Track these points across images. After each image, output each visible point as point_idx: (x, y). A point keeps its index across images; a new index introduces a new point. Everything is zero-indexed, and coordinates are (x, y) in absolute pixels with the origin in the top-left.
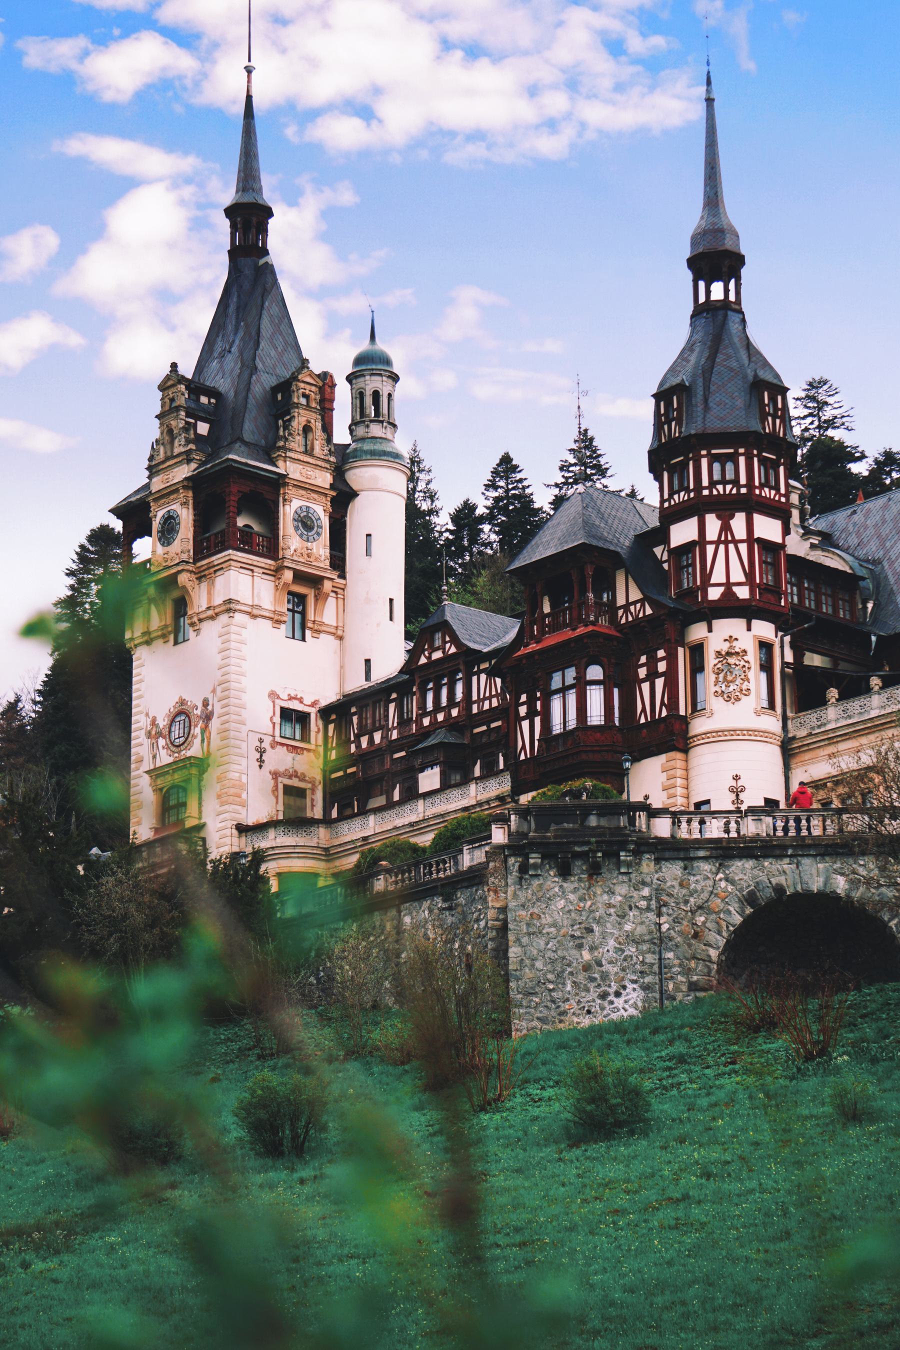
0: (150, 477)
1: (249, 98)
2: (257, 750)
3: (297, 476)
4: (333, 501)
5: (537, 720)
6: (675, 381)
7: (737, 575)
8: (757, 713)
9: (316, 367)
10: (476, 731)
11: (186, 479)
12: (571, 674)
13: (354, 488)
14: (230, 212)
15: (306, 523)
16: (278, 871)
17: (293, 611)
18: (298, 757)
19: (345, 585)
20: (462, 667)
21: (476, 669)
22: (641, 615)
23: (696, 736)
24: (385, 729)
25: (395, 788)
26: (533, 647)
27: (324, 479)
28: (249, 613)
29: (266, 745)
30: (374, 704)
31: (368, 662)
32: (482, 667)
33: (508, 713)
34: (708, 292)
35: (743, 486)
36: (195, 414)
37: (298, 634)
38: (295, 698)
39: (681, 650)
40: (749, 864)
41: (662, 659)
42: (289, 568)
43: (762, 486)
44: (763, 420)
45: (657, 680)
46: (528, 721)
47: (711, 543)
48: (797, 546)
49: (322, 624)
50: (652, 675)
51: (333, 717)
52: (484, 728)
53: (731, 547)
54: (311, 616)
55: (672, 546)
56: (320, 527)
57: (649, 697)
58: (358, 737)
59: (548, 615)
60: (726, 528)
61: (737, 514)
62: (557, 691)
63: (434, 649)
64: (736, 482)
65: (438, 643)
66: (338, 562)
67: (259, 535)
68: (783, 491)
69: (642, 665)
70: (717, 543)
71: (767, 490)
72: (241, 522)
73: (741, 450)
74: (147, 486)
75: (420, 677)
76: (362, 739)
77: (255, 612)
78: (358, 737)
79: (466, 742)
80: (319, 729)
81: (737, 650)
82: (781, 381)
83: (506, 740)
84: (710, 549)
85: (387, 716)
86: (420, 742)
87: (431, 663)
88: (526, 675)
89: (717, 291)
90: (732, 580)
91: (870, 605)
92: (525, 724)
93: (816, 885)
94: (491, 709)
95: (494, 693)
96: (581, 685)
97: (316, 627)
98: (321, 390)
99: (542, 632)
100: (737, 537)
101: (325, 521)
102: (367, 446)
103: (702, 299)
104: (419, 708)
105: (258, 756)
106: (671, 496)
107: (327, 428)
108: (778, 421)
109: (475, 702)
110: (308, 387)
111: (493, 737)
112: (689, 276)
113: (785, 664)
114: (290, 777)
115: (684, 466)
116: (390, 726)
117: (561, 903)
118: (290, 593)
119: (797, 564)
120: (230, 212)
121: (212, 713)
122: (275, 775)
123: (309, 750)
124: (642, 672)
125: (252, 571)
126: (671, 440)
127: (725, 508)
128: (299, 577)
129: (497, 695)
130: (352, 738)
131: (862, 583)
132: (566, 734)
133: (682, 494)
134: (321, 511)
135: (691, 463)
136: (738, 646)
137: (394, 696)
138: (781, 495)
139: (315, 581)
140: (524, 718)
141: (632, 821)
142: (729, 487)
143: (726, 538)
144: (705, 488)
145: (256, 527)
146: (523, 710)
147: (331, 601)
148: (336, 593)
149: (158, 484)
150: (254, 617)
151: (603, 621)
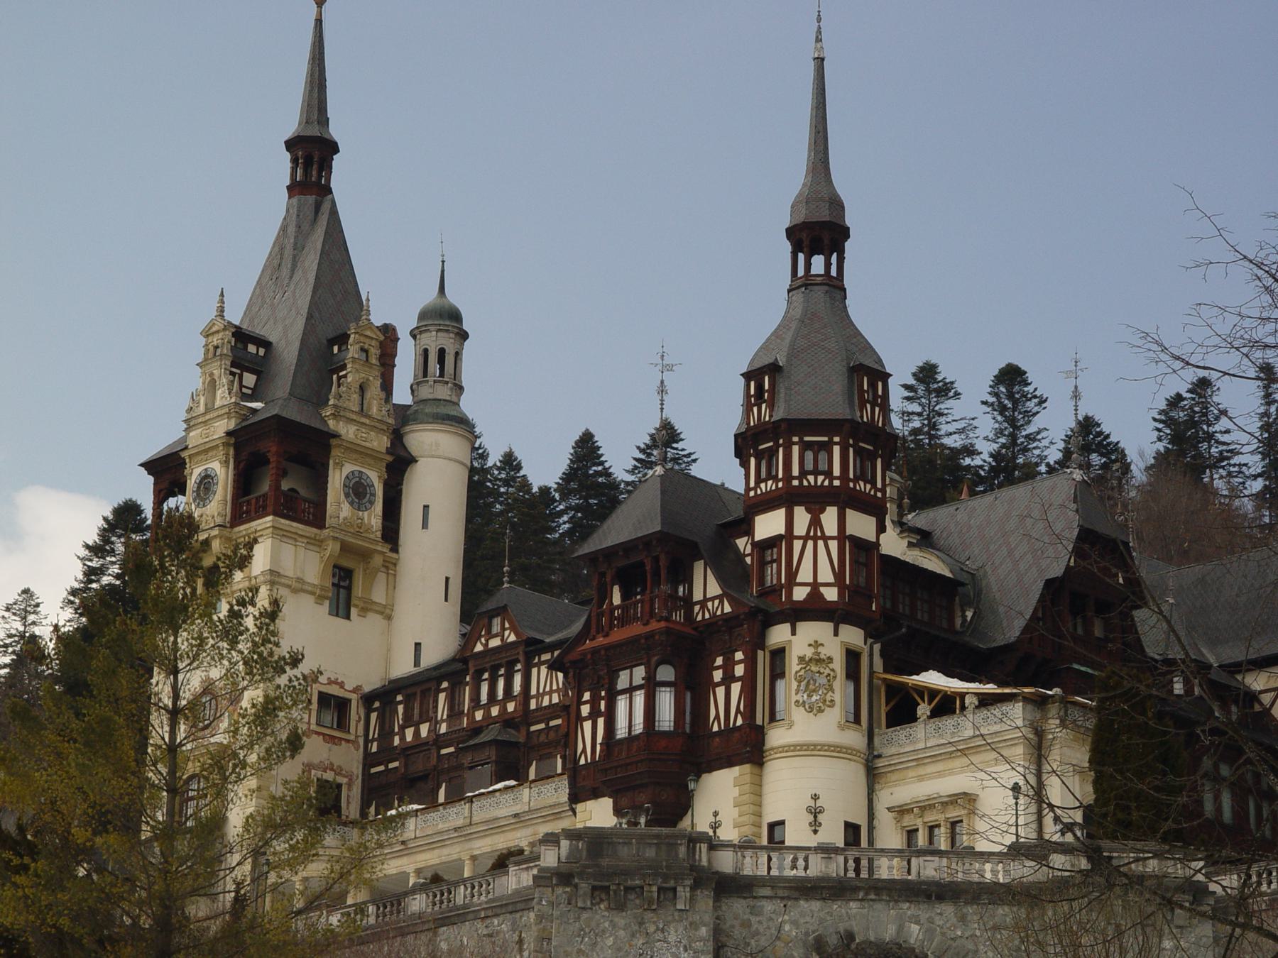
0: (187, 430)
1: (319, 22)
3: (351, 436)
4: (390, 467)
5: (601, 721)
6: (768, 360)
7: (826, 575)
8: (841, 727)
9: (378, 318)
10: (533, 728)
11: (229, 434)
12: (639, 673)
14: (290, 145)
15: (358, 491)
18: (335, 748)
20: (521, 658)
22: (719, 613)
23: (772, 749)
25: (439, 787)
26: (601, 640)
27: (380, 443)
28: (289, 586)
31: (418, 645)
33: (568, 711)
34: (808, 265)
35: (837, 478)
36: (239, 364)
38: (336, 682)
39: (760, 653)
40: (815, 905)
41: (740, 662)
42: (335, 538)
43: (856, 480)
44: (862, 407)
45: (733, 685)
46: (590, 722)
47: (799, 538)
48: (893, 544)
50: (729, 679)
51: (377, 704)
52: (542, 726)
53: (820, 543)
54: (358, 590)
55: (757, 539)
56: (374, 495)
57: (725, 704)
58: (403, 728)
59: (618, 607)
60: (816, 522)
61: (828, 508)
62: (623, 692)
63: (490, 636)
64: (828, 474)
65: (496, 628)
66: (391, 533)
67: (306, 500)
68: (879, 485)
69: (718, 668)
70: (805, 539)
71: (862, 484)
72: (285, 486)
73: (837, 439)
74: (184, 439)
77: (294, 585)
78: (403, 728)
79: (522, 740)
81: (822, 656)
82: (883, 366)
83: (567, 740)
84: (797, 545)
85: (436, 707)
86: (471, 737)
87: (488, 652)
88: (591, 673)
89: (818, 264)
90: (820, 580)
91: (969, 614)
92: (587, 725)
93: (889, 933)
94: (551, 706)
95: (555, 687)
96: (651, 686)
98: (382, 345)
99: (611, 626)
100: (827, 534)
102: (429, 409)
103: (801, 272)
104: (471, 700)
107: (387, 387)
108: (877, 409)
109: (534, 697)
110: (367, 341)
112: (787, 247)
113: (872, 673)
115: (772, 453)
117: (610, 941)
119: (891, 563)
120: (290, 145)
123: (348, 741)
124: (718, 675)
125: (296, 540)
126: (760, 423)
127: (815, 500)
129: (558, 690)
131: (960, 589)
132: (631, 739)
133: (770, 483)
134: (375, 478)
135: (781, 450)
136: (824, 652)
137: (445, 685)
138: (877, 490)
139: (365, 556)
140: (586, 719)
141: (692, 851)
142: (820, 478)
143: (815, 533)
144: (795, 478)
145: (303, 492)
146: (585, 710)
147: (381, 577)
148: (387, 568)
149: (195, 438)
150: (295, 591)
151: (678, 616)
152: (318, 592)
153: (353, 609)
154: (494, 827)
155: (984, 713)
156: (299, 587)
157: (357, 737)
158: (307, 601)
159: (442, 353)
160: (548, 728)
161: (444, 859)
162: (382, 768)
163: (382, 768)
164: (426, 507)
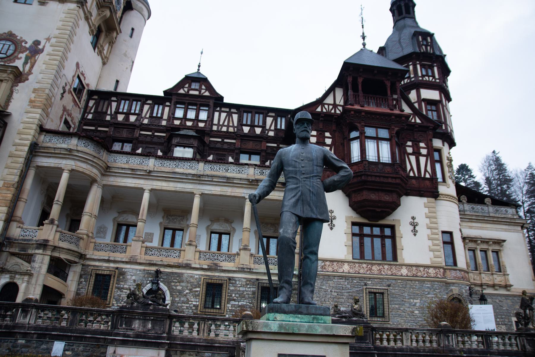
16: (74, 168)
18: (74, 107)
19: (115, 42)
21: (218, 109)
24: (139, 115)
28: (85, 13)
29: (67, 88)
31: (117, 82)
32: (223, 109)
49: (104, 50)
50: (417, 154)
51: (96, 97)
52: (220, 140)
63: (190, 89)
69: (409, 146)
76: (119, 115)
87: (187, 95)
94: (227, 132)
95: (231, 124)
101: (122, 7)
105: (62, 92)
106: (423, 76)
111: (225, 146)
116: (143, 115)
121: (42, 51)
122: (65, 109)
123: (79, 107)
124: (410, 150)
130: (109, 112)
150: (87, 19)
154: (229, 181)
155: (497, 208)
160: (223, 142)
161: (178, 189)
162: (93, 128)
163: (93, 128)
164: (133, 29)
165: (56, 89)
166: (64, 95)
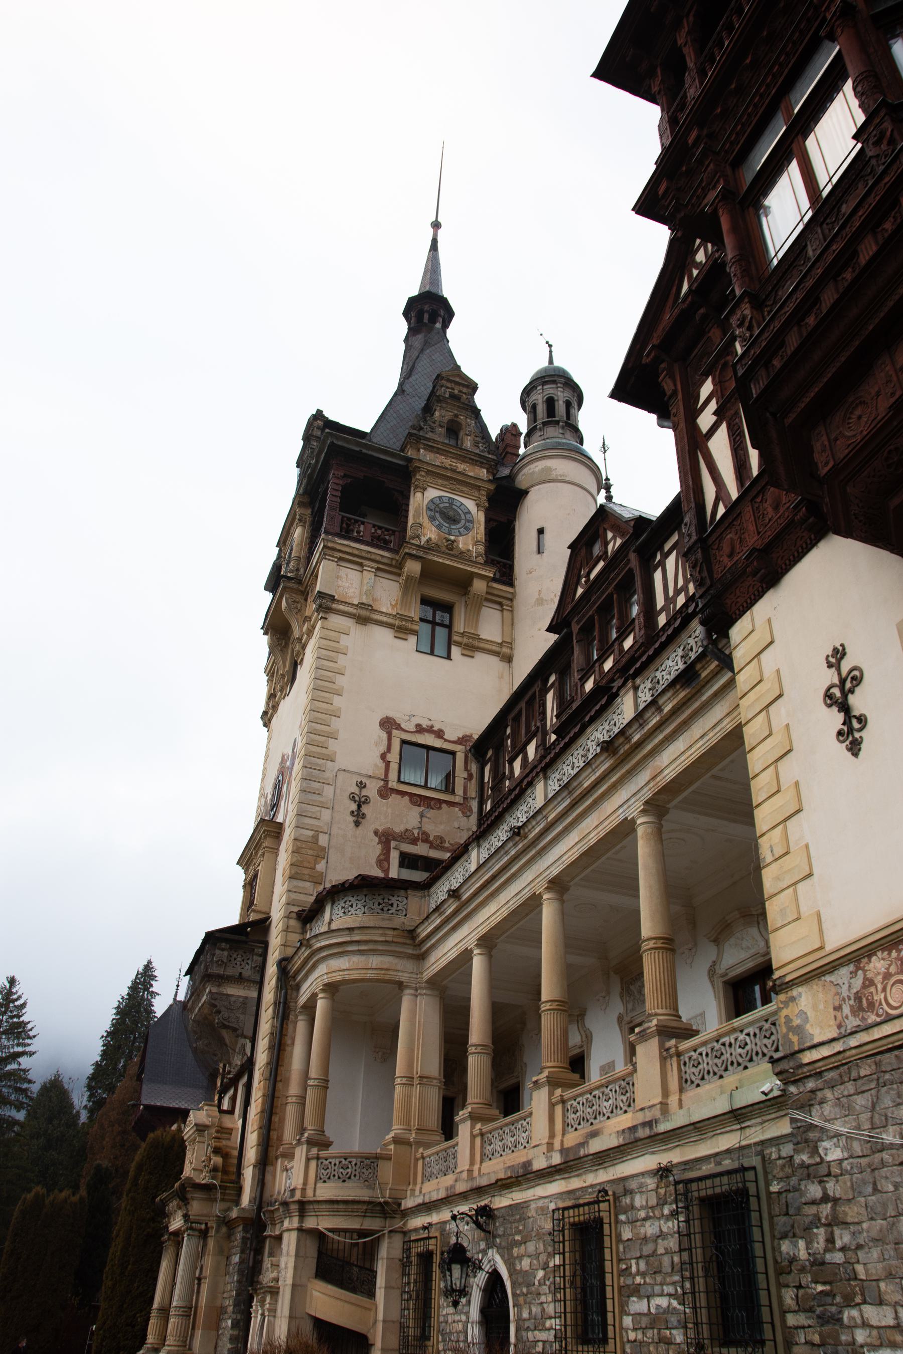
2: (352, 798)
4: (490, 499)
13: (523, 488)
15: (448, 515)
17: (433, 623)
18: (431, 813)
19: (514, 594)
29: (372, 790)
30: (530, 703)
37: (440, 649)
38: (430, 730)
49: (477, 637)
54: (460, 625)
75: (578, 622)
77: (364, 613)
80: (470, 777)
85: (544, 713)
97: (465, 640)
105: (354, 807)
114: (414, 841)
118: (425, 601)
122: (386, 838)
125: (361, 565)
128: (430, 574)
139: (462, 583)
148: (501, 604)
150: (363, 621)
152: (397, 622)
153: (454, 648)
156: (364, 616)
157: (465, 798)
158: (383, 635)
159: (550, 403)
164: (541, 531)
165: (326, 815)
166: (365, 809)
